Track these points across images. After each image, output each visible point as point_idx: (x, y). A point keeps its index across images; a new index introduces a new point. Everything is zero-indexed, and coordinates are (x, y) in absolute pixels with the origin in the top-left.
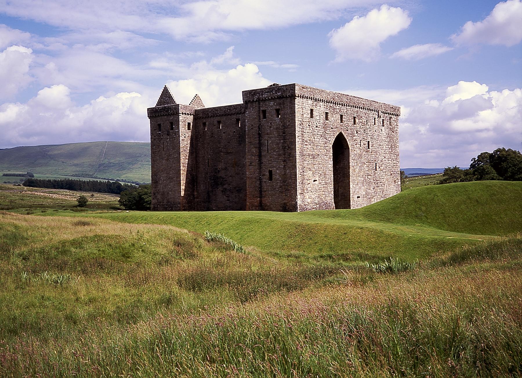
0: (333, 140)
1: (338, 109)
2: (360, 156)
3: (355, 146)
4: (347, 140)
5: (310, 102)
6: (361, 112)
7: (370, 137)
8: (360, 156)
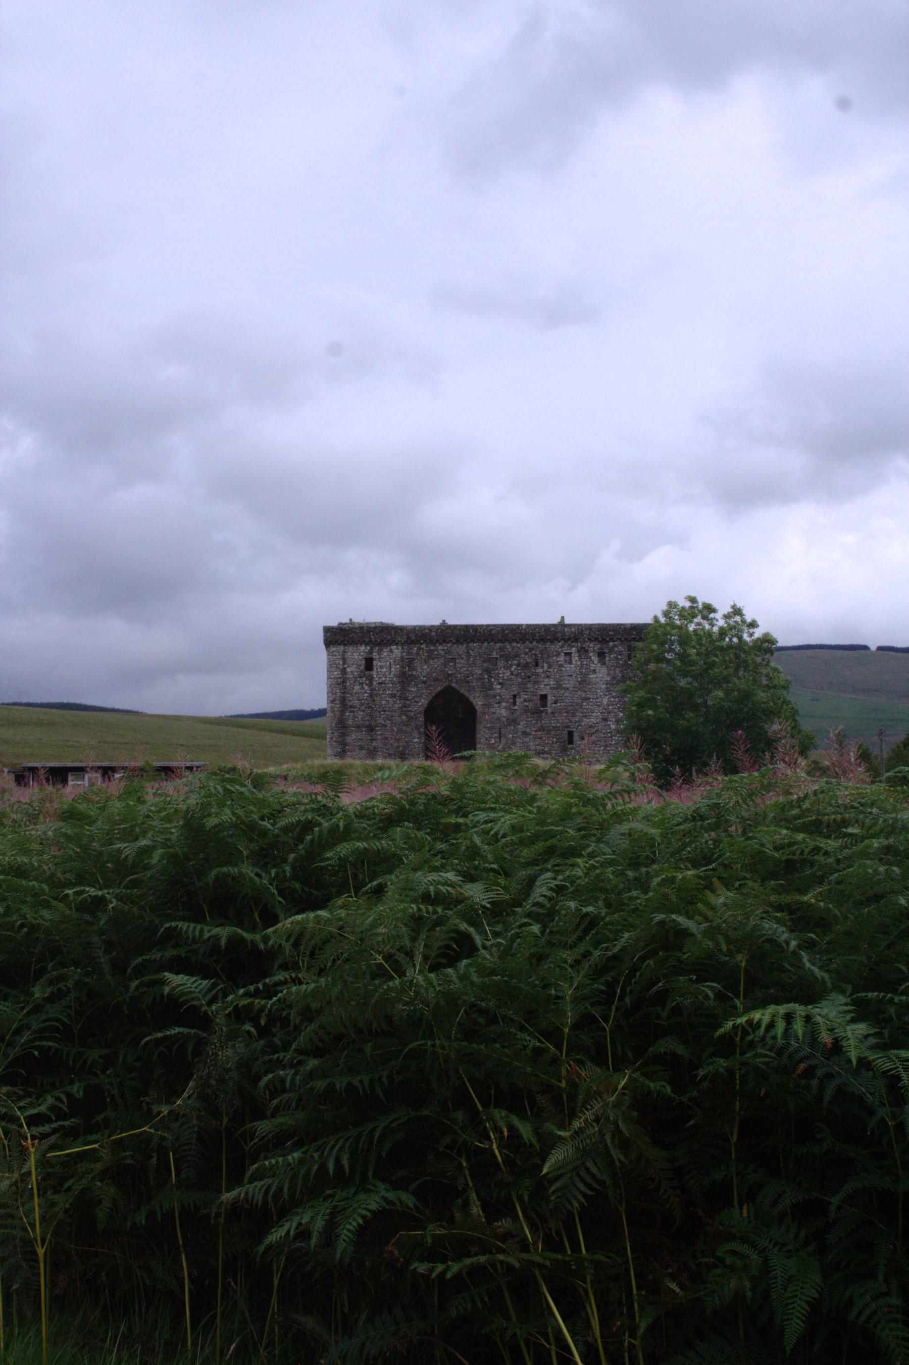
0: (424, 702)
1: (443, 650)
2: (513, 722)
3: (497, 705)
4: (471, 698)
5: (363, 648)
6: (513, 648)
7: (548, 687)
8: (513, 722)
